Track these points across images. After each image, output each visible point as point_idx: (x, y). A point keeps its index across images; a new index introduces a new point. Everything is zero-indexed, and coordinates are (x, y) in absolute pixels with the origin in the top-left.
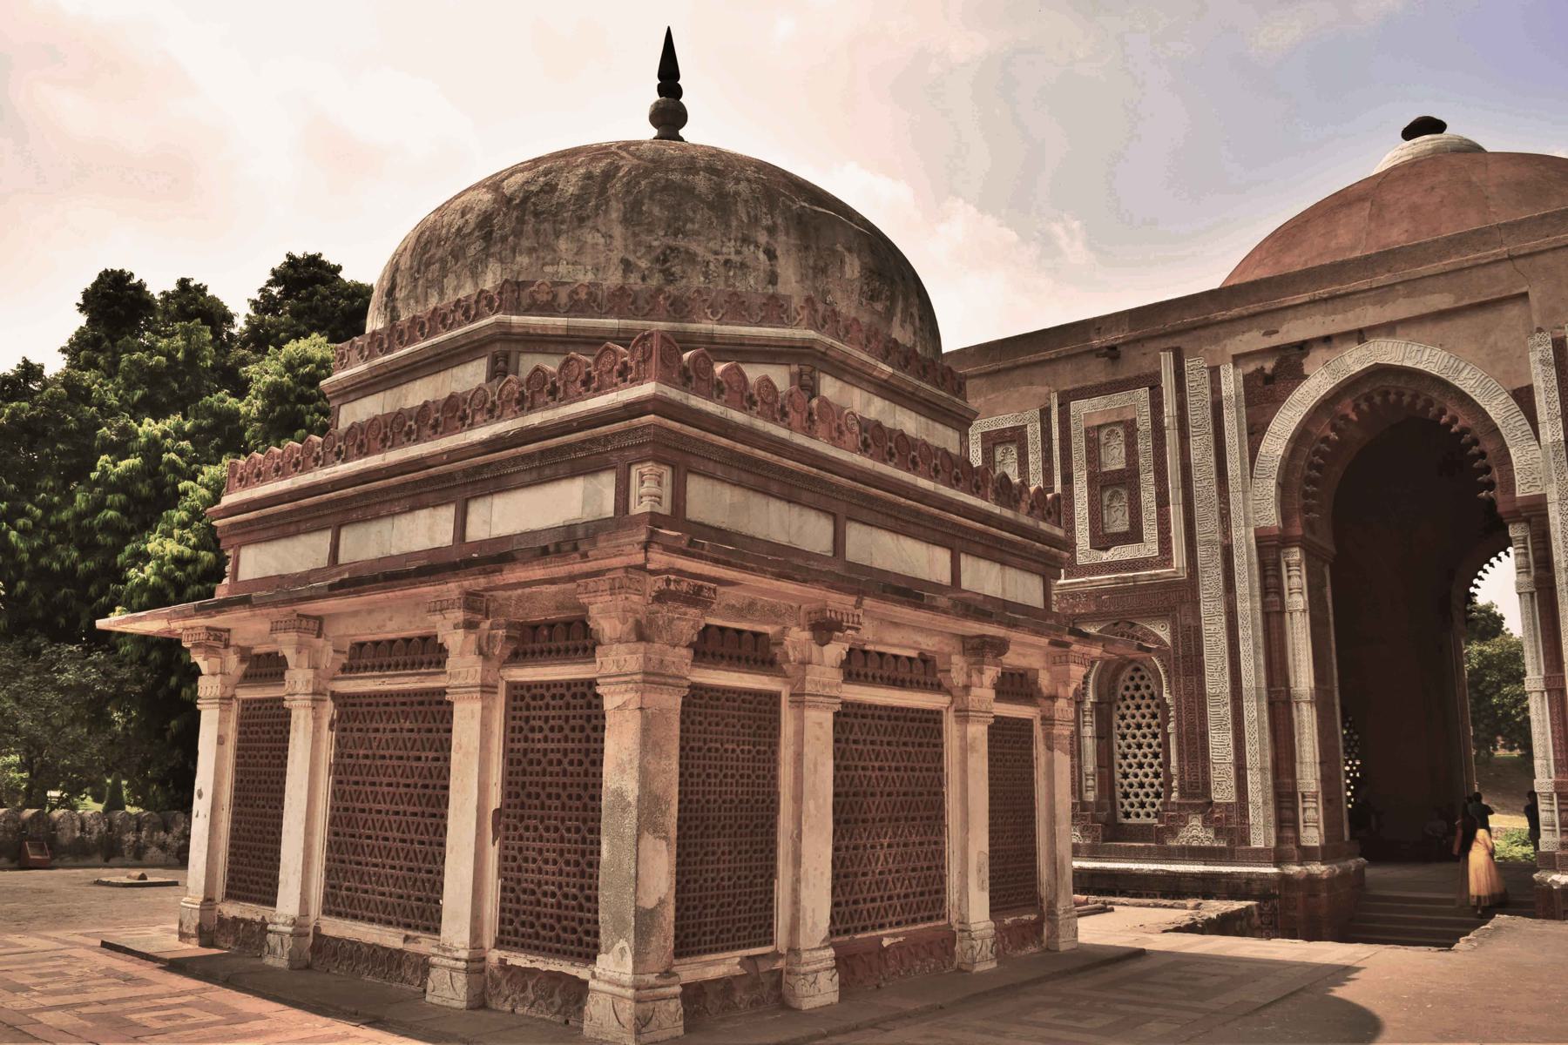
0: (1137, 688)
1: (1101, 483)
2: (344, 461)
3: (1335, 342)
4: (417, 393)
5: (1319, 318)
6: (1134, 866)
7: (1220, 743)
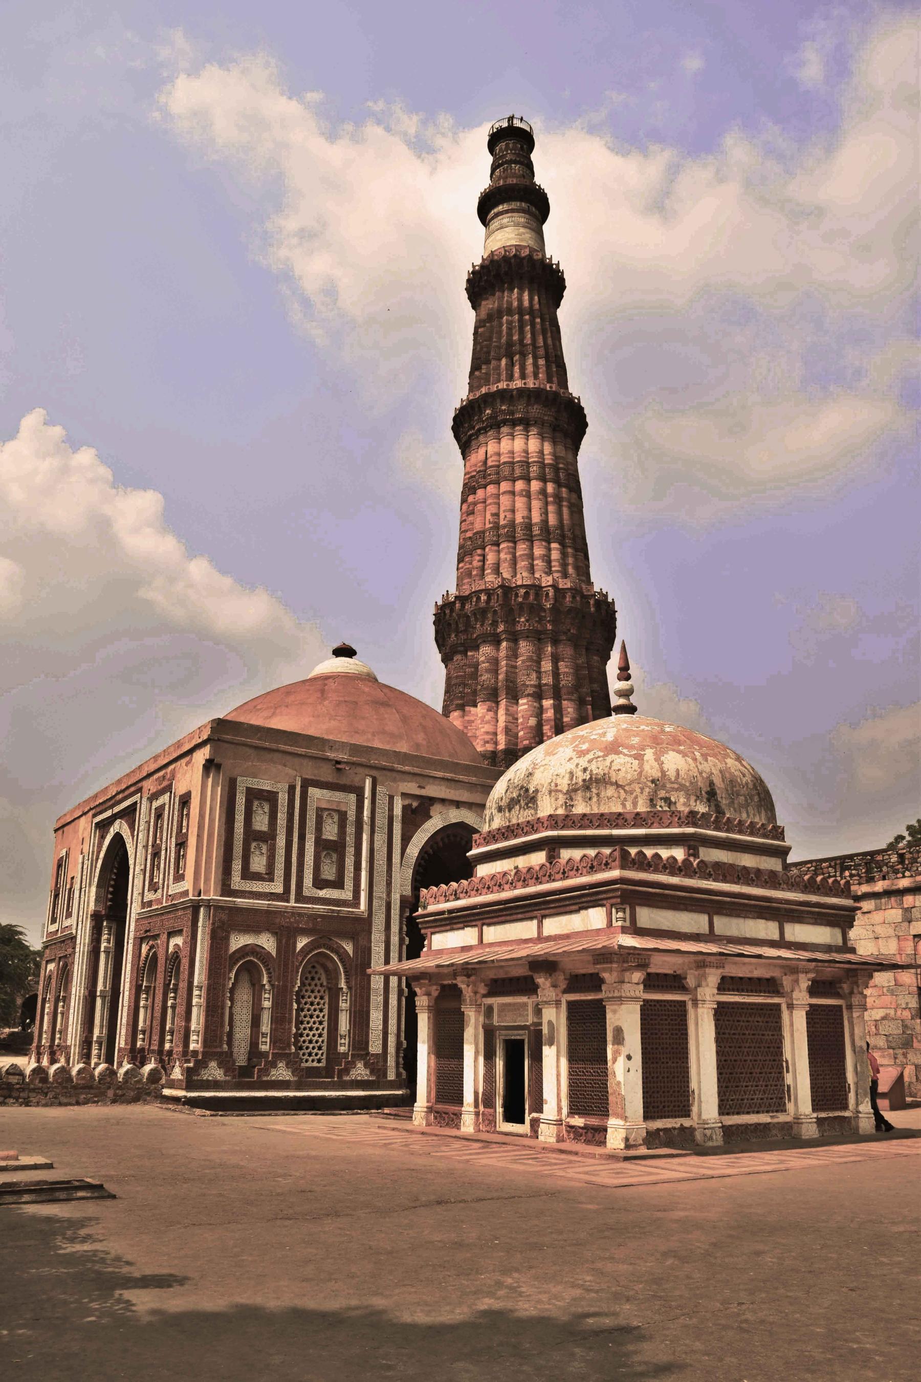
0: (313, 979)
1: (322, 845)
2: (714, 880)
3: (447, 803)
4: (748, 861)
5: (443, 788)
6: (327, 1094)
7: (376, 1017)
